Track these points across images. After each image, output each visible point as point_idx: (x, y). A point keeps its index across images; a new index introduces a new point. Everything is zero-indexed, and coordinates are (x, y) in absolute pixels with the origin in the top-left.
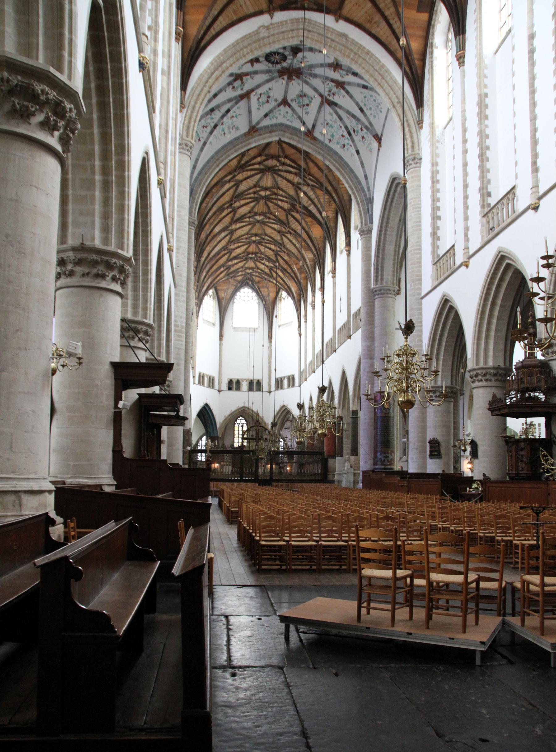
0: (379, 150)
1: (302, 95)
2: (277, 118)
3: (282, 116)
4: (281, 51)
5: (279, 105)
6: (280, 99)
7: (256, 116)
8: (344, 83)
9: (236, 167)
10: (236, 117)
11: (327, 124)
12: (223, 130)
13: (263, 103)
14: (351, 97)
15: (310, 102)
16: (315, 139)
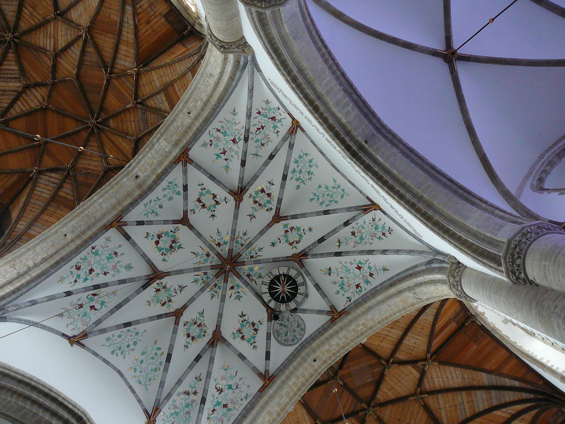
0: (64, 335)
1: (174, 245)
2: (164, 190)
3: (165, 202)
4: (292, 305)
5: (185, 213)
6: (190, 216)
7: (196, 177)
8: (177, 323)
9: (92, 38)
10: (218, 156)
11: (116, 253)
12: (225, 134)
13: (201, 194)
14: (151, 319)
15: (160, 249)
16: (107, 227)
